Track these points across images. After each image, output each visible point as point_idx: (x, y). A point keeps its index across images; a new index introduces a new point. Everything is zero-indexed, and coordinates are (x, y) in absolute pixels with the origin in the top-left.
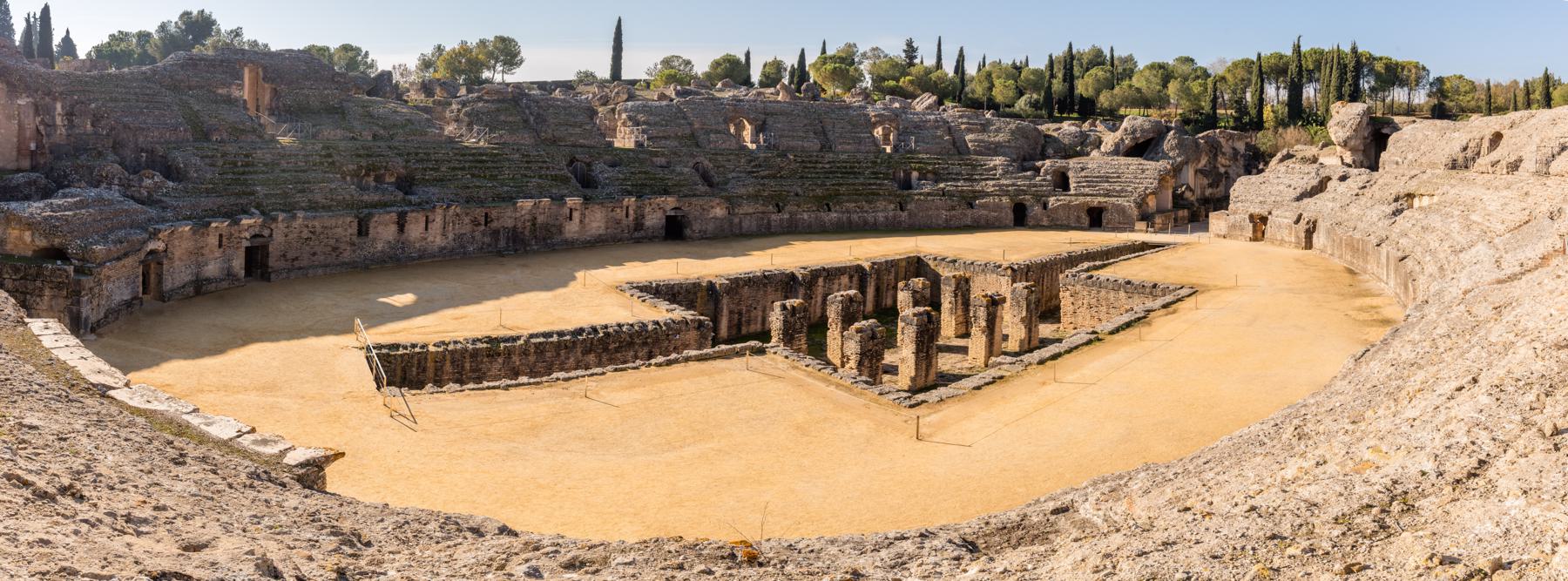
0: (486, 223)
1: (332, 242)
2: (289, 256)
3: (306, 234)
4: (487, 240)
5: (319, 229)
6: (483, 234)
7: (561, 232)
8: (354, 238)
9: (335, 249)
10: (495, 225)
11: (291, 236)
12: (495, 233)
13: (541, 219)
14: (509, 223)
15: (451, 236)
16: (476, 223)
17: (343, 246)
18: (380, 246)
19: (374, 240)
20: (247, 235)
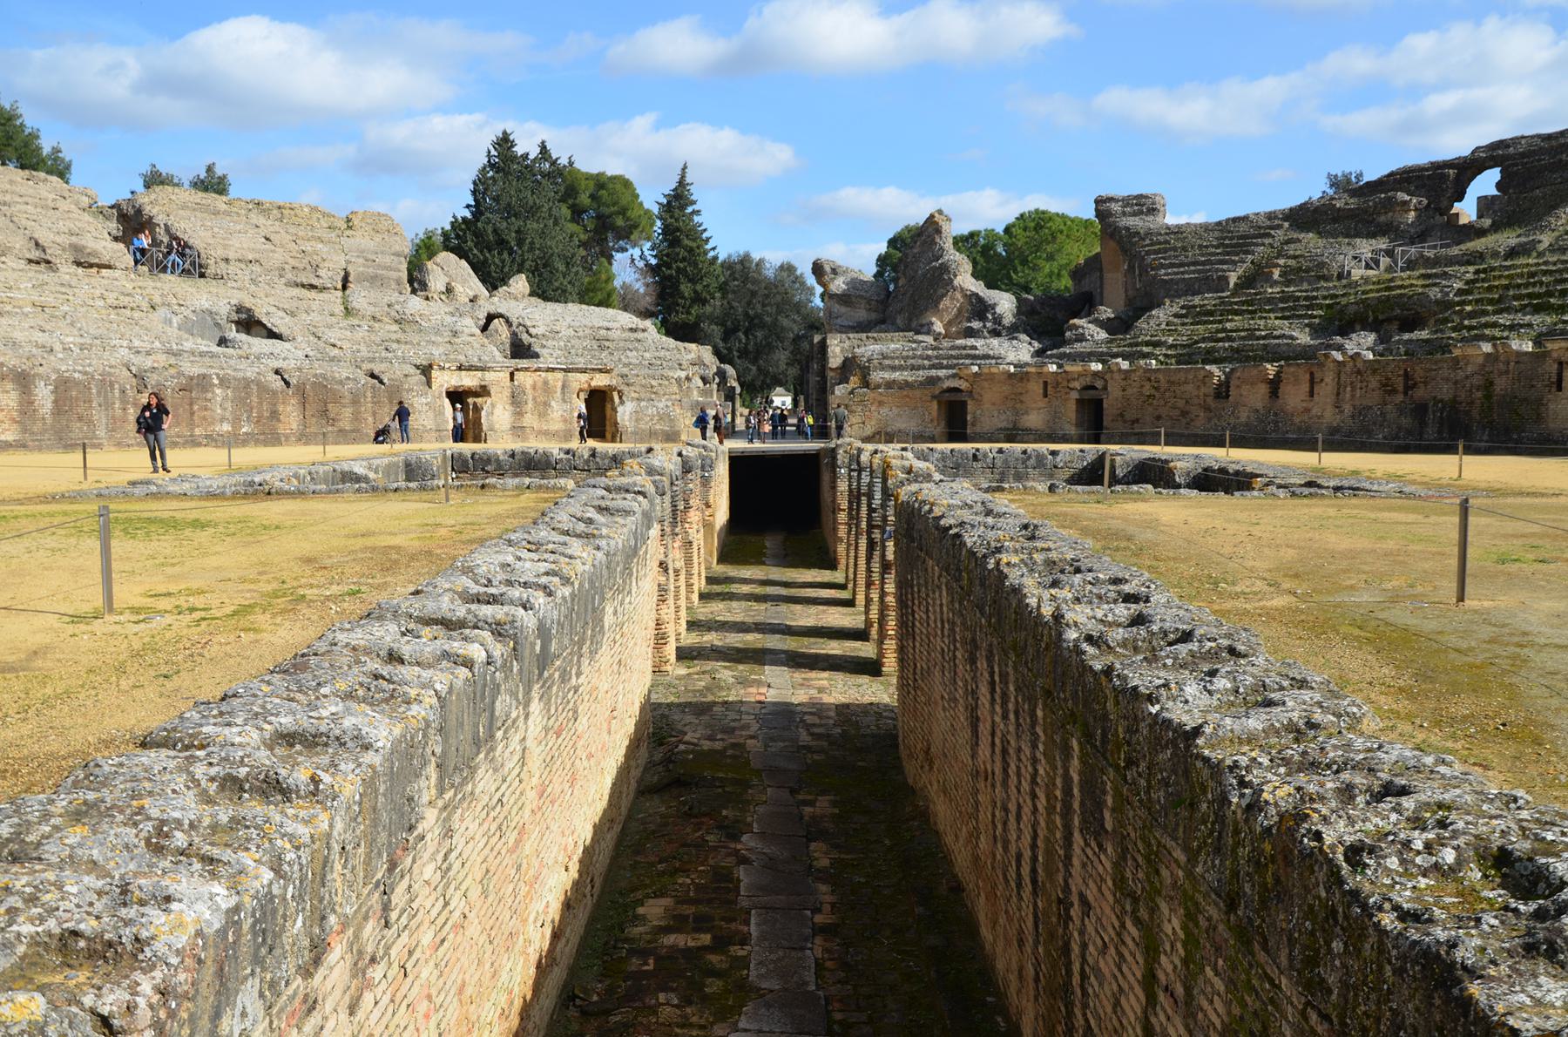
0: (1406, 393)
1: (1181, 403)
2: (1128, 416)
3: (1147, 390)
4: (1406, 421)
5: (1164, 385)
6: (1401, 410)
7: (1539, 418)
8: (1210, 400)
9: (1184, 413)
10: (1420, 393)
11: (1129, 391)
12: (1420, 410)
13: (1501, 384)
14: (1445, 392)
15: (1347, 409)
16: (1387, 388)
17: (1195, 411)
18: (1244, 416)
19: (1236, 406)
20: (1077, 385)
